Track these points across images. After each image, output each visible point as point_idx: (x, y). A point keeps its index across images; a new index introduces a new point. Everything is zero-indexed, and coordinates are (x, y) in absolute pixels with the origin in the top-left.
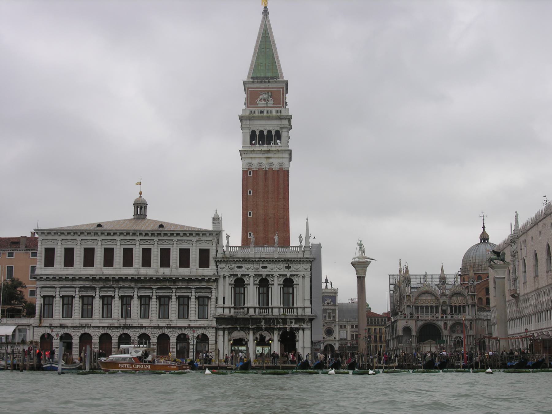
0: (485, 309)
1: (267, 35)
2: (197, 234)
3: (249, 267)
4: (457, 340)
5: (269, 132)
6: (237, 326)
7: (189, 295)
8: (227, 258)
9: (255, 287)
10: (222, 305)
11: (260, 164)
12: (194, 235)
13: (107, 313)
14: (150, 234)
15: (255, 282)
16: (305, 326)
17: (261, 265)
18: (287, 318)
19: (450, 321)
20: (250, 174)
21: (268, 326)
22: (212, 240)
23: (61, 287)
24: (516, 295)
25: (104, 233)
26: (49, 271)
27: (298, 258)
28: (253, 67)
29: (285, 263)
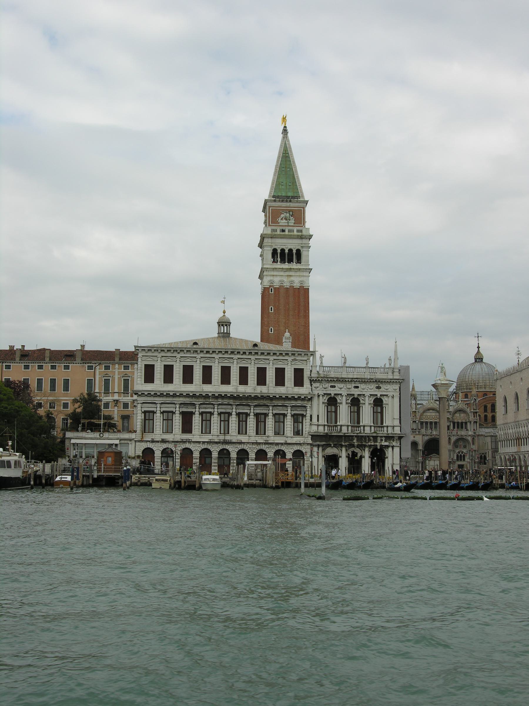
0: (483, 425)
1: (287, 155)
3: (342, 386)
4: (459, 455)
5: (290, 250)
6: (331, 443)
7: (286, 412)
8: (322, 377)
9: (347, 406)
10: (317, 423)
11: (282, 282)
13: (206, 429)
14: (247, 353)
17: (354, 385)
18: (378, 436)
20: (271, 291)
21: (360, 444)
23: (162, 403)
25: (203, 351)
26: (149, 387)
28: (274, 186)
29: (376, 383)
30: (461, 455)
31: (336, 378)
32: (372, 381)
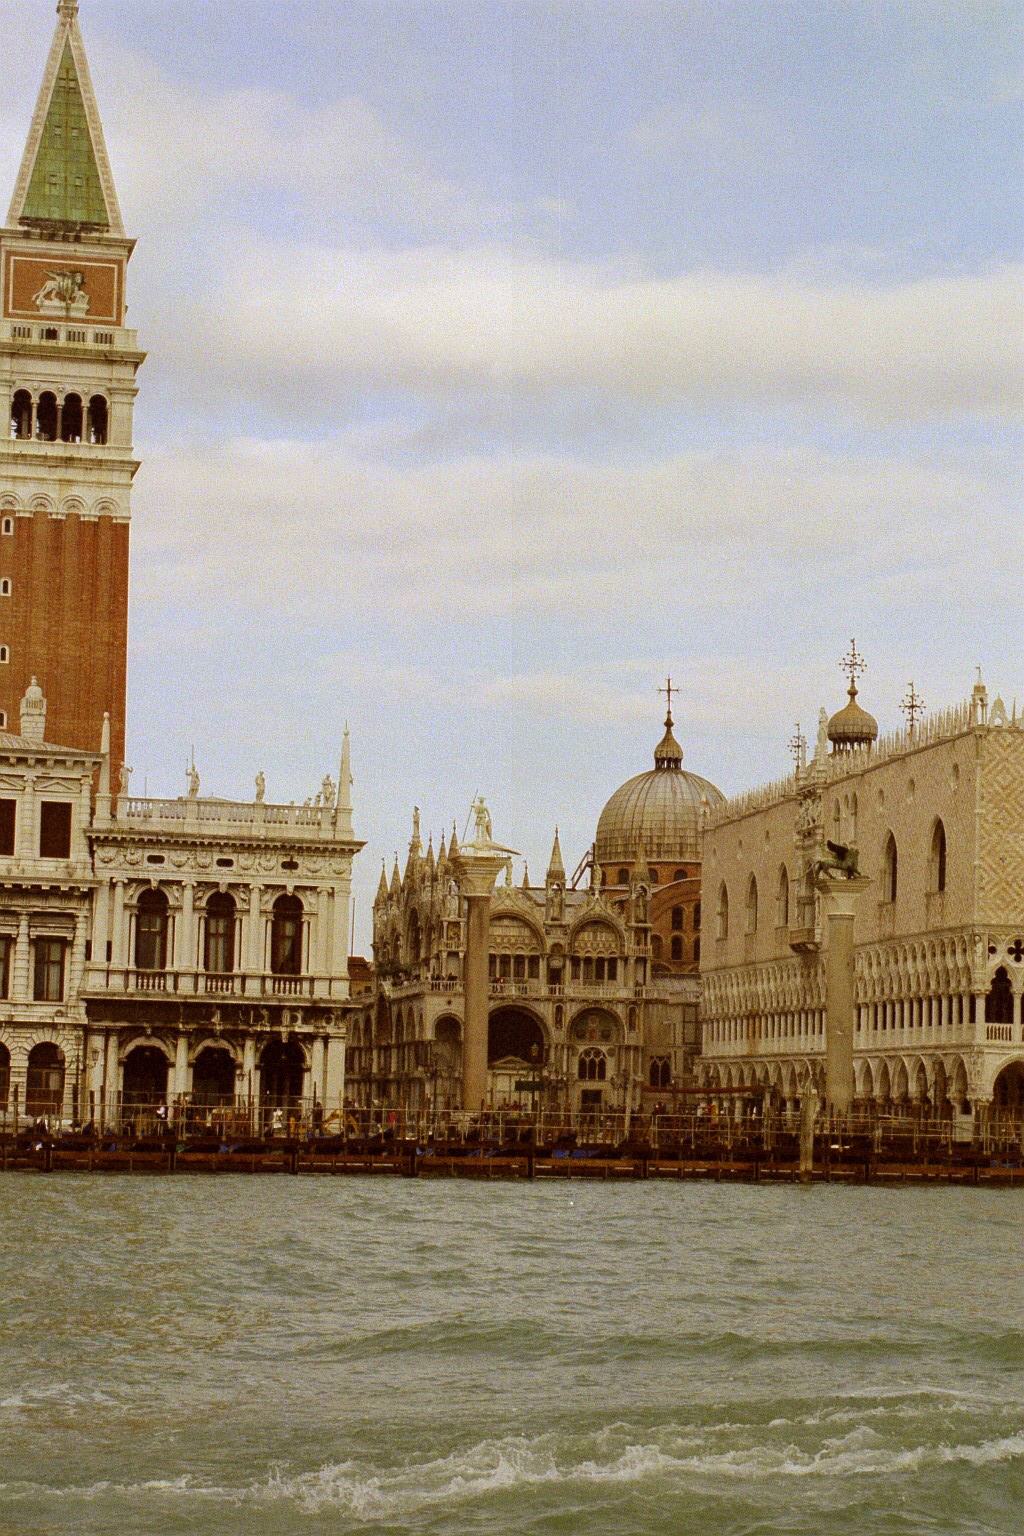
0: (669, 970)
1: (72, 84)
2: (57, 762)
3: (183, 859)
5: (73, 399)
6: (145, 1025)
7: (12, 931)
9: (197, 916)
10: (104, 966)
11: (41, 501)
12: (31, 762)
15: (197, 903)
16: (331, 1029)
17: (217, 857)
18: (282, 1008)
19: (574, 1003)
20: (7, 530)
22: (79, 780)
24: (811, 947)
27: (319, 843)
28: (27, 184)
30: (592, 1061)
31: (165, 834)
32: (271, 845)
